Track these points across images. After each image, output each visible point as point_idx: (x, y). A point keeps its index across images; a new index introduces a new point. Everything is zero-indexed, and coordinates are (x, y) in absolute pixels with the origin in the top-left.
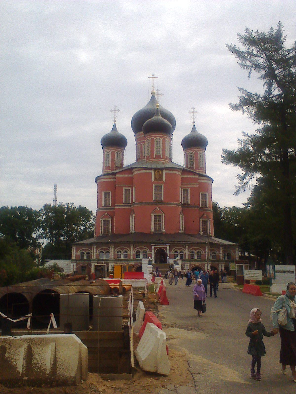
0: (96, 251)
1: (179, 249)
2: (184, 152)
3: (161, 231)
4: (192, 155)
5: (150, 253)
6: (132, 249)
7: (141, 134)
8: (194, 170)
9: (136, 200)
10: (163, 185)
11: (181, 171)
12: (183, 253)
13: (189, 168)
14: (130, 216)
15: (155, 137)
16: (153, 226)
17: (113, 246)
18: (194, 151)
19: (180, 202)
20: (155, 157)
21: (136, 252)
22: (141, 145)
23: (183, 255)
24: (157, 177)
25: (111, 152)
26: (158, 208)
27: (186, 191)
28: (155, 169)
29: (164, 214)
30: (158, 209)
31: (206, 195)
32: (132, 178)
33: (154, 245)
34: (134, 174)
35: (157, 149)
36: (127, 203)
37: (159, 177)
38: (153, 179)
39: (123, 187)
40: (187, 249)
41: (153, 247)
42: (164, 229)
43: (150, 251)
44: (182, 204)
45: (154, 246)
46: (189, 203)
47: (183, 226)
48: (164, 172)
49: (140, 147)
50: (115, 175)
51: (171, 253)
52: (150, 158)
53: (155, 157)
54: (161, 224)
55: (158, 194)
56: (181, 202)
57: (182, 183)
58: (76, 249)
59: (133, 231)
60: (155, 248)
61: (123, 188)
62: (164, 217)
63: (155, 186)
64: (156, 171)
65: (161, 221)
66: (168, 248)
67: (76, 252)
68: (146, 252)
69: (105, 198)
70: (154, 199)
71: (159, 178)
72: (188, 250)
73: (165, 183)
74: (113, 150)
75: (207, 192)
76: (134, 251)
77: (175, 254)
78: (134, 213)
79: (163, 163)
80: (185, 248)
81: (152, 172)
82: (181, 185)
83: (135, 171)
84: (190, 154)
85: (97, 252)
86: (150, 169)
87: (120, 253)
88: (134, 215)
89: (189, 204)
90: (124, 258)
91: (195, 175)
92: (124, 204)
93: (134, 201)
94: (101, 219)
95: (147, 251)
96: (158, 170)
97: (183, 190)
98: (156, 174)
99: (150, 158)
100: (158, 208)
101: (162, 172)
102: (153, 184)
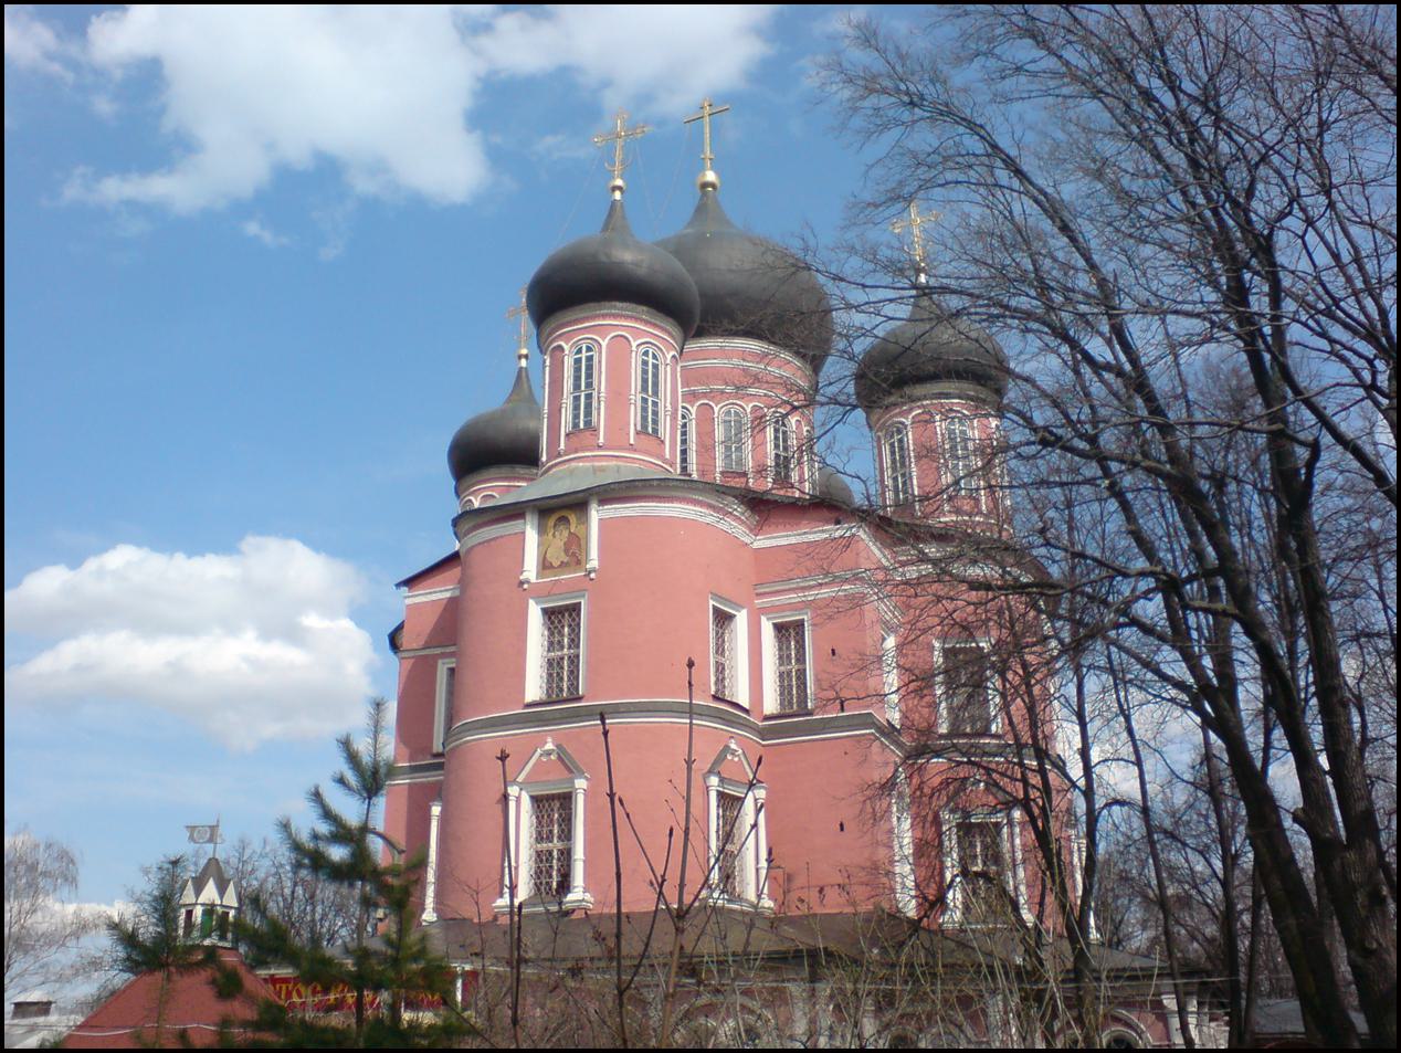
15: (567, 336)
20: (562, 446)
24: (557, 555)
27: (788, 632)
30: (549, 753)
35: (577, 399)
37: (566, 551)
38: (530, 570)
39: (444, 655)
48: (596, 514)
53: (562, 446)
61: (440, 662)
63: (549, 613)
64: (551, 522)
71: (566, 559)
91: (838, 522)
102: (532, 603)
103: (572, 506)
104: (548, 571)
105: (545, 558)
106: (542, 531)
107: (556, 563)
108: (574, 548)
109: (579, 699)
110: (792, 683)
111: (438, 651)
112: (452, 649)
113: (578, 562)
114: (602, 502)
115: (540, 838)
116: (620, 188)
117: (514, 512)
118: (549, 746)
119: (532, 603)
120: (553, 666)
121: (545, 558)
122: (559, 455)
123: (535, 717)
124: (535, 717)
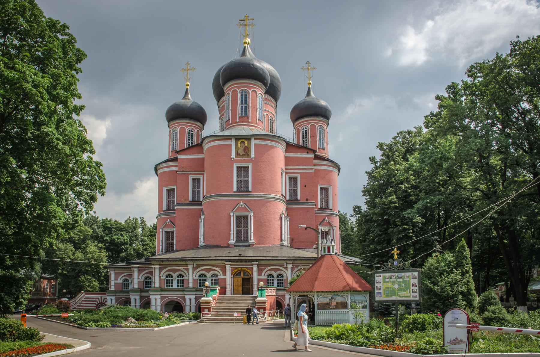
0: (138, 276)
1: (276, 270)
3: (248, 241)
4: (306, 131)
5: (224, 277)
6: (191, 271)
10: (251, 164)
11: (285, 144)
12: (283, 276)
14: (200, 221)
16: (233, 234)
17: (157, 267)
18: (307, 123)
19: (282, 195)
21: (200, 276)
23: (282, 280)
24: (241, 152)
25: (179, 129)
26: (242, 203)
27: (293, 180)
28: (238, 138)
29: (252, 214)
30: (242, 206)
32: (203, 159)
33: (230, 263)
37: (244, 151)
38: (233, 155)
39: (190, 174)
40: (289, 270)
41: (228, 268)
42: (252, 238)
43: (223, 275)
44: (287, 201)
45: (230, 265)
46: (299, 198)
47: (289, 236)
48: (253, 142)
51: (260, 277)
54: (247, 230)
56: (284, 195)
57: (286, 165)
58: (115, 274)
59: (202, 244)
60: (232, 270)
61: (190, 176)
62: (252, 218)
63: (238, 167)
64: (239, 142)
65: (248, 227)
66: (255, 268)
67: (116, 279)
68: (217, 276)
70: (235, 189)
71: (244, 153)
72: (292, 271)
73: (255, 162)
74: (182, 125)
75: (330, 185)
76: (194, 275)
77: (268, 280)
78: (203, 214)
80: (286, 268)
81: (233, 142)
82: (286, 169)
84: (303, 129)
85: (140, 277)
86: (229, 138)
87: (171, 279)
88: (203, 217)
89: (299, 201)
90: (178, 286)
91: (308, 153)
92: (190, 202)
94: (161, 230)
95: (219, 274)
96: (241, 140)
97: (289, 178)
98: (239, 147)
100: (242, 203)
101: (249, 144)
102: (234, 164)
104: (239, 156)
105: (237, 152)
107: (241, 154)
108: (247, 151)
110: (293, 192)
111: (189, 173)
112: (203, 173)
113: (248, 155)
114: (255, 139)
115: (237, 226)
120: (239, 182)
121: (237, 152)
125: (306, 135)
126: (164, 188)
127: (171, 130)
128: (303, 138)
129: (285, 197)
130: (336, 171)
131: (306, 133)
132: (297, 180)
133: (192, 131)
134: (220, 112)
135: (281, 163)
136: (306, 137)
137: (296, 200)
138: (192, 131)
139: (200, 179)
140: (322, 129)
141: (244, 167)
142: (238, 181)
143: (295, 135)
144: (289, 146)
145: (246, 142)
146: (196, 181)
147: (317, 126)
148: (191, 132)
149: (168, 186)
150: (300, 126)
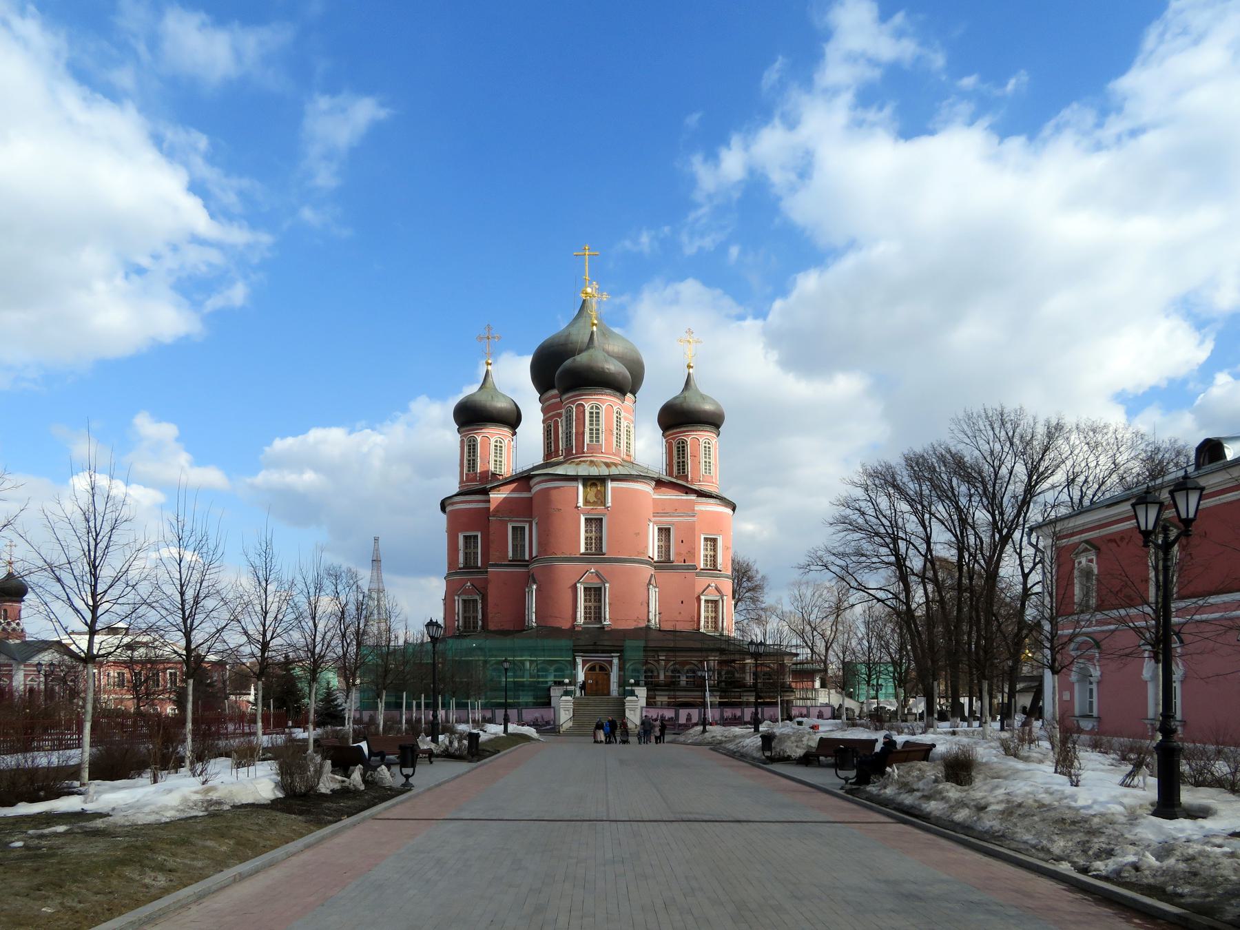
2: (664, 440)
4: (683, 447)
7: (554, 397)
8: (687, 481)
9: (539, 552)
11: (653, 483)
13: (676, 477)
19: (649, 557)
22: (556, 423)
24: (592, 498)
27: (665, 532)
30: (592, 573)
31: (714, 541)
32: (531, 498)
34: (536, 489)
35: (592, 430)
36: (518, 559)
38: (581, 503)
44: (655, 562)
48: (610, 485)
49: (552, 426)
50: (489, 495)
52: (574, 452)
53: (585, 449)
55: (594, 537)
56: (651, 556)
63: (586, 519)
64: (589, 483)
69: (466, 547)
70: (583, 550)
79: (608, 465)
83: (536, 484)
91: (687, 493)
92: (510, 561)
93: (534, 555)
99: (574, 452)
102: (582, 515)
103: (600, 481)
104: (588, 504)
105: (586, 499)
106: (585, 486)
109: (604, 554)
110: (665, 549)
111: (508, 519)
116: (596, 325)
117: (574, 478)
118: (592, 570)
119: (582, 515)
121: (586, 499)
122: (584, 453)
123: (583, 559)
124: (583, 559)
125: (684, 454)
126: (460, 534)
127: (465, 440)
128: (679, 458)
129: (653, 559)
130: (729, 511)
131: (683, 450)
132: (670, 532)
133: (501, 442)
134: (544, 411)
135: (649, 510)
136: (684, 457)
137: (669, 561)
138: (501, 442)
139: (524, 527)
140: (709, 444)
141: (596, 519)
142: (586, 538)
143: (664, 456)
144: (659, 483)
145: (599, 485)
146: (518, 531)
147: (701, 441)
148: (498, 444)
149: (467, 531)
150: (673, 439)
